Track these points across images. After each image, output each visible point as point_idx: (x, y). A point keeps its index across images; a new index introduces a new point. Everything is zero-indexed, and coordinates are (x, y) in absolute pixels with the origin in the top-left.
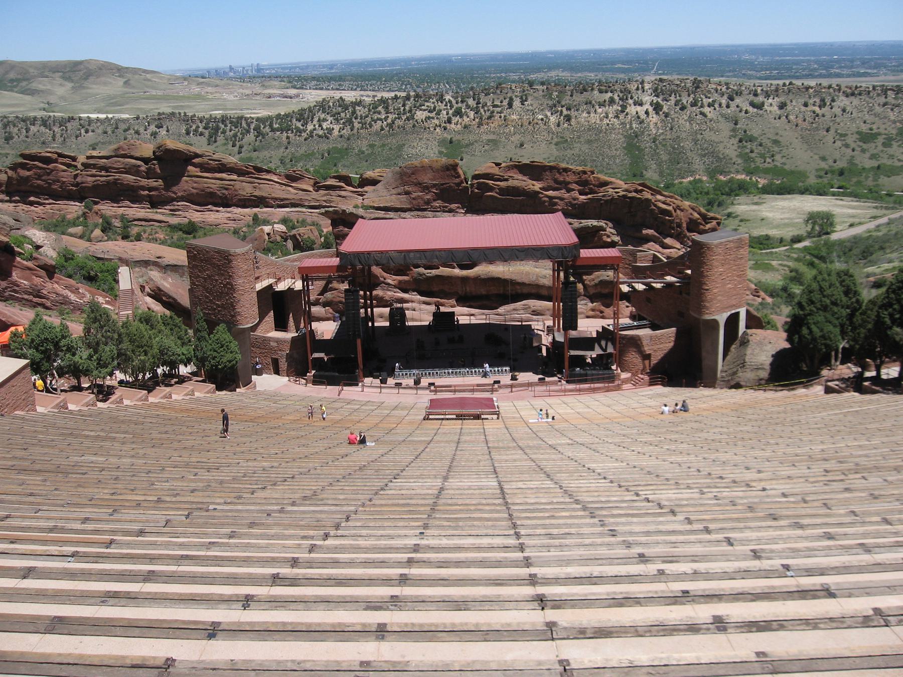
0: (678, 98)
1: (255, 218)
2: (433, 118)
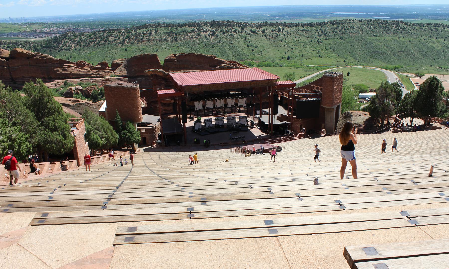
1: (66, 83)
2: (117, 40)
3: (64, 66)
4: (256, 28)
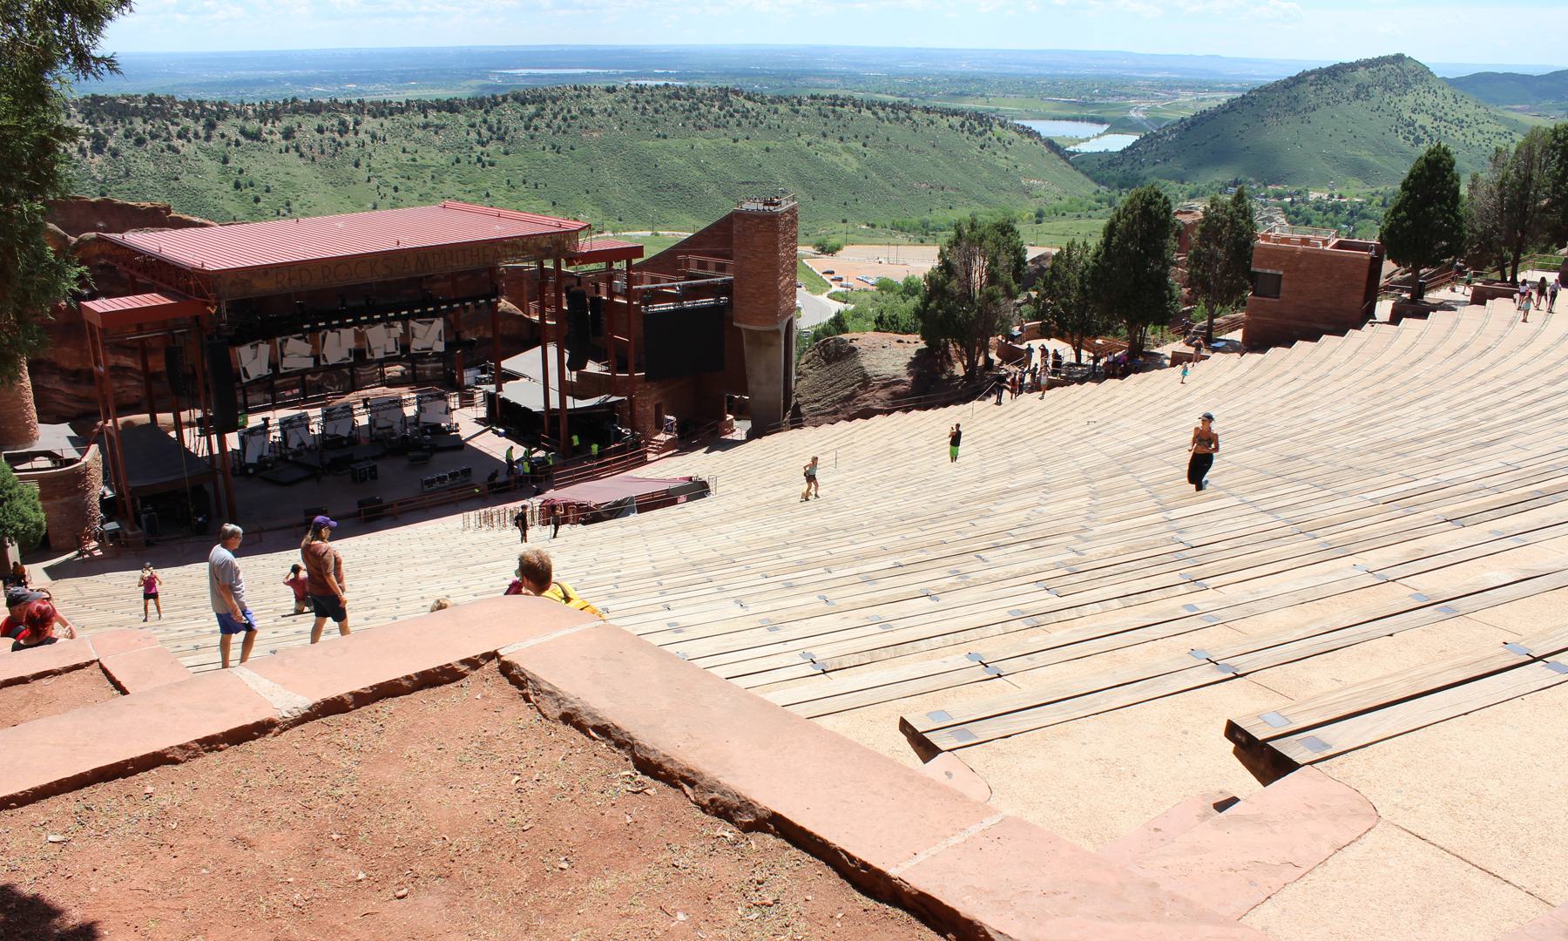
0: (129, 127)
4: (261, 122)
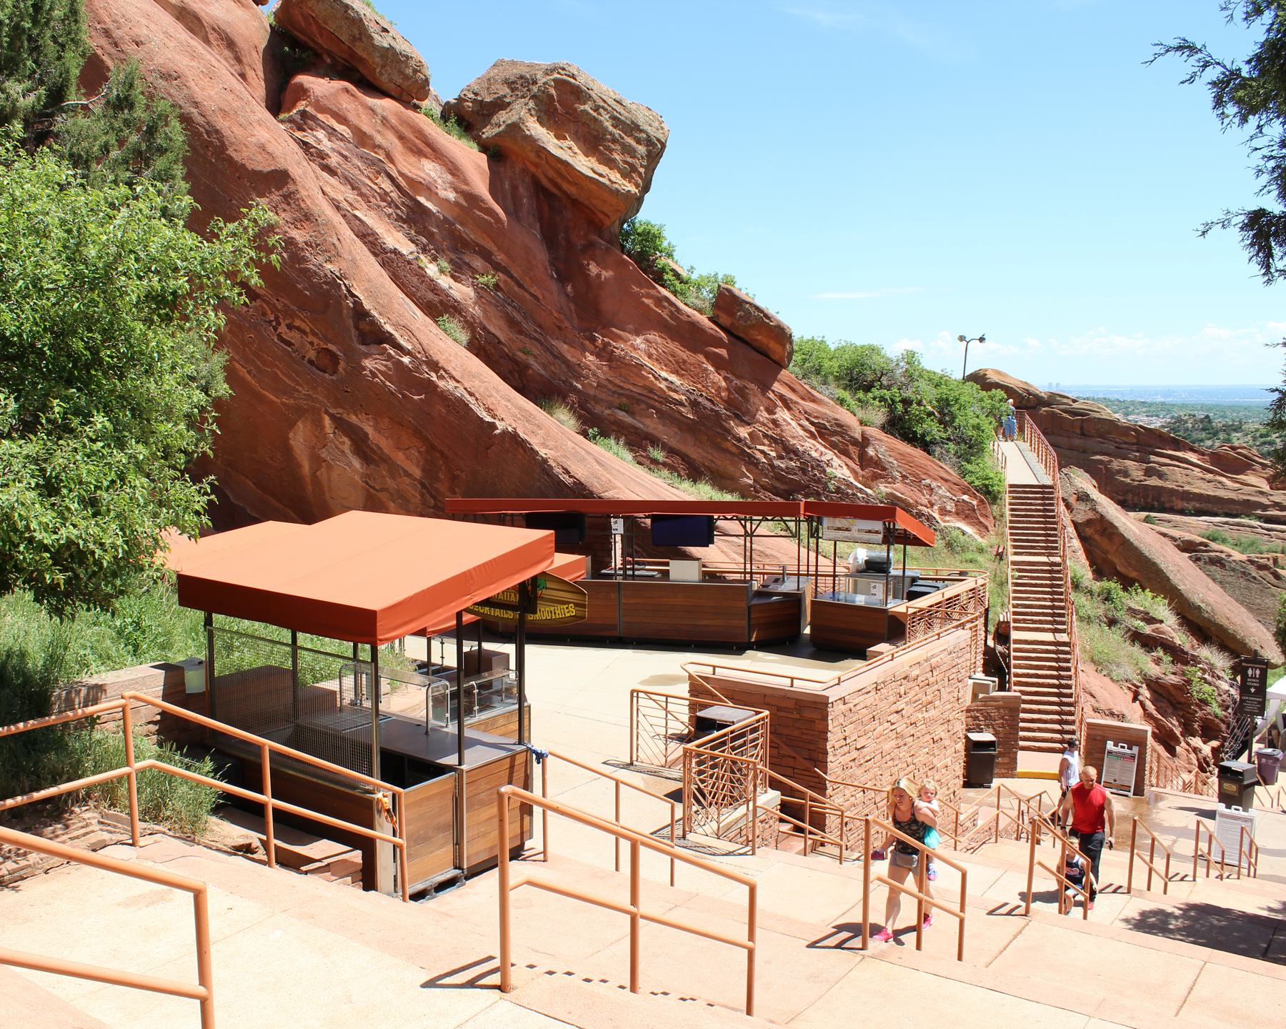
3: (1153, 458)
